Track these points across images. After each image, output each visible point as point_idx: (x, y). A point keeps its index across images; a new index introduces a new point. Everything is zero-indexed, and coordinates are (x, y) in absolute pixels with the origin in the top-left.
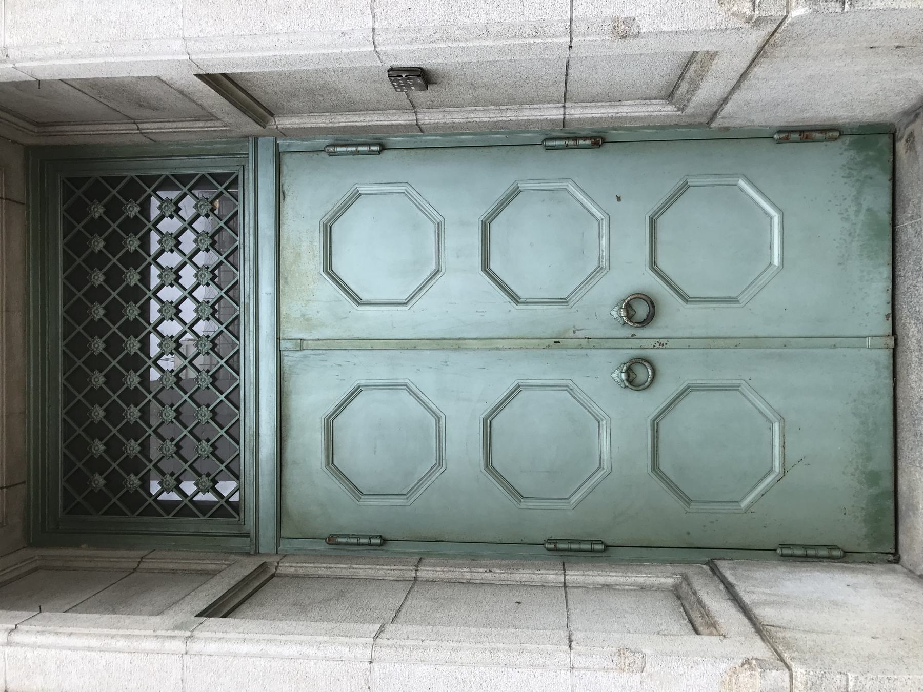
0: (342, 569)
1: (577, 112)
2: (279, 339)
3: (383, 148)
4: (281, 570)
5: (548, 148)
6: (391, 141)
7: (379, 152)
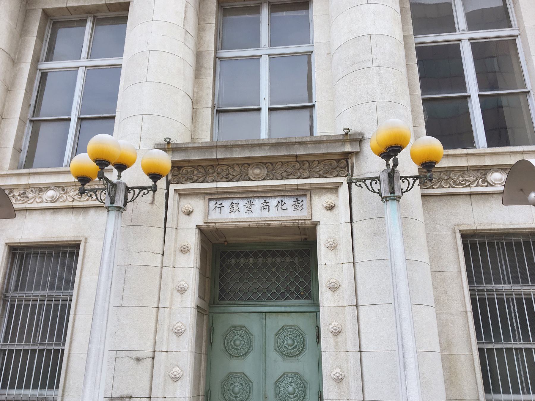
0: (204, 333)
2: (265, 312)
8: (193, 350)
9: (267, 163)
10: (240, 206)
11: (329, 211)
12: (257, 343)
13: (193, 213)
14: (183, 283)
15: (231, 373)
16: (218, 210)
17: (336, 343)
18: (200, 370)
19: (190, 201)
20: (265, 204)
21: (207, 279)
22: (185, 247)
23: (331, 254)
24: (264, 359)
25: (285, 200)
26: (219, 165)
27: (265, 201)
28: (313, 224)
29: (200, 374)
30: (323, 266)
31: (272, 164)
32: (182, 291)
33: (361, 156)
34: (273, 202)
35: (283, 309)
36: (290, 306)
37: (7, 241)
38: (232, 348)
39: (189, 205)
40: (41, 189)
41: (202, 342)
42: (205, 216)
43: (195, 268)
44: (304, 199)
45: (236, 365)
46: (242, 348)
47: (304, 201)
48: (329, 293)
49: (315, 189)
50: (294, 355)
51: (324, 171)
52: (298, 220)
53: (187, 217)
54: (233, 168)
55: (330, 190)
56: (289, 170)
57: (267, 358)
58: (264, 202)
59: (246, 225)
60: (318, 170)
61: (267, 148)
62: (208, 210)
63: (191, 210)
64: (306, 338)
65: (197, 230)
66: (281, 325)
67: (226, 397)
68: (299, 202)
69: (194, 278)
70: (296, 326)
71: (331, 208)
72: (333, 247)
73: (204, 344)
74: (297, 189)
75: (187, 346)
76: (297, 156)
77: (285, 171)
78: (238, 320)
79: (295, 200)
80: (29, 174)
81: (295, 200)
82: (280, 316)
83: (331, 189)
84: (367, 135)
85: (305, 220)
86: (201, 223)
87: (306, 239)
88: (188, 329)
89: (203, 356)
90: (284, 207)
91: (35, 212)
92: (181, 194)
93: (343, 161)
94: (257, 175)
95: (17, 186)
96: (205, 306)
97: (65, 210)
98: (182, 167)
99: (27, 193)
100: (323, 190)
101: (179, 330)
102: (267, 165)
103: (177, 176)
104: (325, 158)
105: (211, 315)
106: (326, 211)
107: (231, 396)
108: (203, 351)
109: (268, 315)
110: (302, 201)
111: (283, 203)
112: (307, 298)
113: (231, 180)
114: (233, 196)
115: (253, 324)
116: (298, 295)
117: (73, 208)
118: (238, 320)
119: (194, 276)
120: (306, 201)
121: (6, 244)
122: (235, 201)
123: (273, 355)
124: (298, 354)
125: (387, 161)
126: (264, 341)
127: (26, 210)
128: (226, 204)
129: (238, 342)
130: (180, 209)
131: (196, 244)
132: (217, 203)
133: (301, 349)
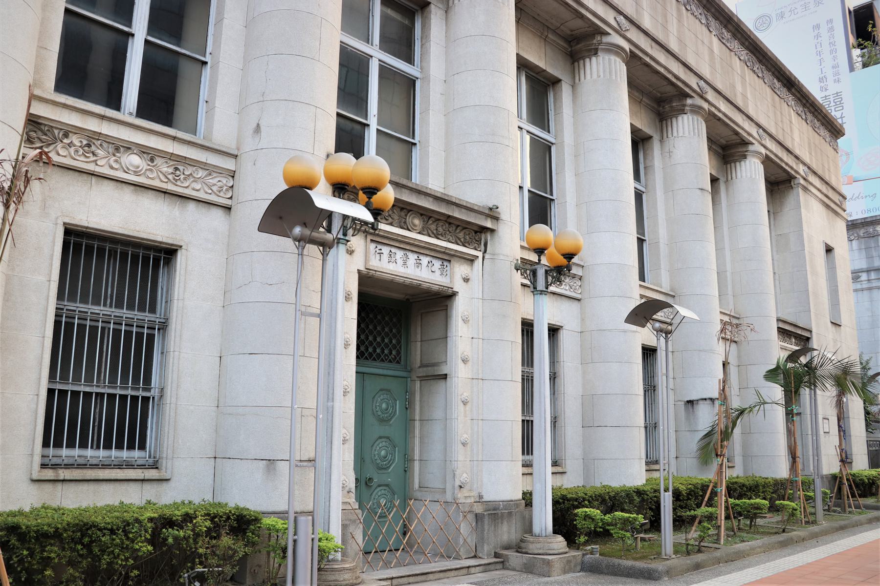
1: (417, 464)
13: (355, 254)
17: (465, 411)
33: (496, 233)
34: (425, 260)
37: (67, 221)
40: (120, 147)
47: (448, 268)
48: (461, 365)
56: (440, 229)
59: (401, 280)
61: (431, 199)
70: (389, 391)
71: (466, 280)
72: (465, 321)
74: (444, 253)
76: (449, 216)
80: (103, 117)
83: (468, 260)
84: (503, 216)
86: (362, 268)
87: (408, 299)
91: (106, 182)
94: (415, 226)
95: (79, 130)
97: (153, 192)
99: (93, 148)
112: (398, 362)
113: (391, 224)
117: (165, 193)
121: (64, 224)
122: (393, 250)
125: (539, 256)
127: (92, 174)
128: (386, 250)
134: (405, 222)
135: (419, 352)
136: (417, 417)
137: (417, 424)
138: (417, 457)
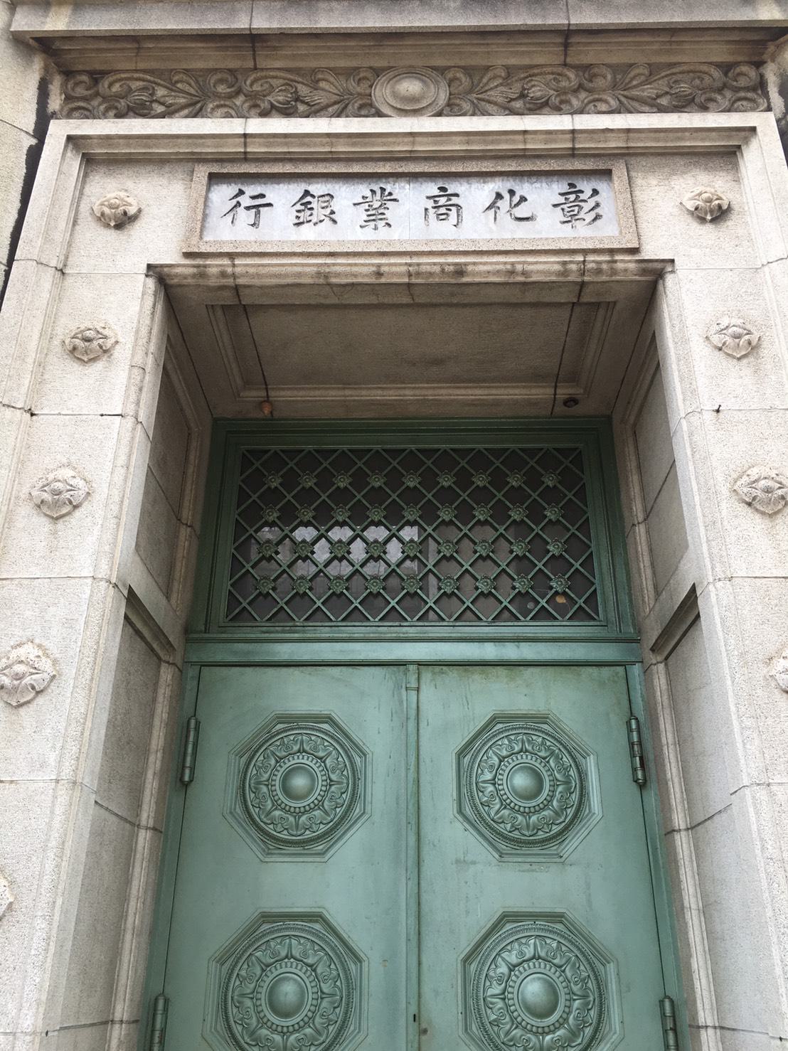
0: (158, 739)
3: (642, 786)
4: (164, 668)
5: (662, 1002)
6: (651, 797)
7: (636, 781)
8: (90, 780)
9: (449, 68)
10: (335, 205)
11: (709, 228)
12: (381, 789)
14: (67, 473)
15: (267, 917)
16: (245, 217)
18: (123, 898)
19: (130, 184)
20: (442, 201)
21: (184, 532)
22: (89, 334)
23: (738, 377)
24: (412, 852)
25: (523, 188)
26: (255, 68)
27: (442, 189)
28: (644, 272)
29: (122, 916)
30: (709, 417)
31: (468, 70)
32: (58, 506)
34: (475, 195)
35: (489, 651)
36: (517, 640)
38: (277, 805)
39: (123, 194)
41: (140, 775)
42: (191, 231)
43: (129, 422)
44: (602, 186)
45: (291, 883)
46: (319, 805)
49: (645, 153)
50: (541, 835)
51: (677, 96)
52: (585, 252)
53: (112, 234)
54: (314, 84)
55: (702, 160)
57: (426, 850)
58: (437, 192)
59: (362, 270)
60: (653, 93)
62: (205, 216)
63: (132, 211)
64: (591, 765)
65: (151, 283)
66: (482, 711)
67: (237, 1029)
68: (582, 196)
69: (122, 459)
70: (543, 719)
71: (717, 214)
73: (151, 784)
74: (573, 154)
75: (52, 758)
77: (522, 96)
78: (302, 694)
79: (566, 189)
81: (566, 189)
82: (477, 679)
85: (612, 251)
86: (168, 254)
87: (571, 401)
88: (69, 672)
89: (144, 839)
90: (519, 212)
92: (93, 157)
93: (744, 69)
96: (171, 625)
98: (104, 73)
100: (677, 159)
101: (19, 677)
102: (450, 75)
103: (85, 99)
104: (674, 59)
105: (192, 672)
106: (695, 225)
107: (263, 1022)
108: (147, 815)
109: (427, 675)
110: (595, 192)
111: (516, 199)
112: (581, 615)
114: (309, 168)
115: (367, 709)
116: (543, 602)
118: (302, 694)
119: (124, 450)
120: (609, 195)
122: (317, 188)
123: (450, 834)
124: (561, 833)
126: (412, 774)
128: (283, 197)
129: (299, 782)
130: (84, 208)
131: (144, 331)
132: (241, 192)
133: (571, 812)
134: (371, 105)
135: (645, 561)
136: (679, 820)
137: (683, 843)
138: (705, 1015)
